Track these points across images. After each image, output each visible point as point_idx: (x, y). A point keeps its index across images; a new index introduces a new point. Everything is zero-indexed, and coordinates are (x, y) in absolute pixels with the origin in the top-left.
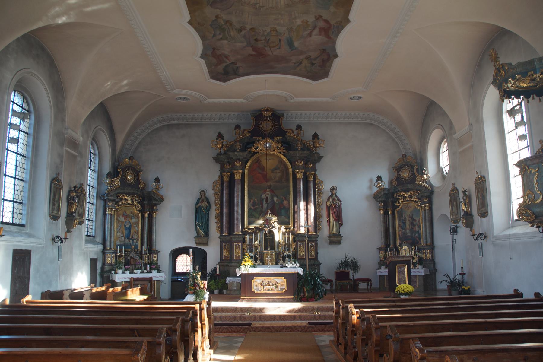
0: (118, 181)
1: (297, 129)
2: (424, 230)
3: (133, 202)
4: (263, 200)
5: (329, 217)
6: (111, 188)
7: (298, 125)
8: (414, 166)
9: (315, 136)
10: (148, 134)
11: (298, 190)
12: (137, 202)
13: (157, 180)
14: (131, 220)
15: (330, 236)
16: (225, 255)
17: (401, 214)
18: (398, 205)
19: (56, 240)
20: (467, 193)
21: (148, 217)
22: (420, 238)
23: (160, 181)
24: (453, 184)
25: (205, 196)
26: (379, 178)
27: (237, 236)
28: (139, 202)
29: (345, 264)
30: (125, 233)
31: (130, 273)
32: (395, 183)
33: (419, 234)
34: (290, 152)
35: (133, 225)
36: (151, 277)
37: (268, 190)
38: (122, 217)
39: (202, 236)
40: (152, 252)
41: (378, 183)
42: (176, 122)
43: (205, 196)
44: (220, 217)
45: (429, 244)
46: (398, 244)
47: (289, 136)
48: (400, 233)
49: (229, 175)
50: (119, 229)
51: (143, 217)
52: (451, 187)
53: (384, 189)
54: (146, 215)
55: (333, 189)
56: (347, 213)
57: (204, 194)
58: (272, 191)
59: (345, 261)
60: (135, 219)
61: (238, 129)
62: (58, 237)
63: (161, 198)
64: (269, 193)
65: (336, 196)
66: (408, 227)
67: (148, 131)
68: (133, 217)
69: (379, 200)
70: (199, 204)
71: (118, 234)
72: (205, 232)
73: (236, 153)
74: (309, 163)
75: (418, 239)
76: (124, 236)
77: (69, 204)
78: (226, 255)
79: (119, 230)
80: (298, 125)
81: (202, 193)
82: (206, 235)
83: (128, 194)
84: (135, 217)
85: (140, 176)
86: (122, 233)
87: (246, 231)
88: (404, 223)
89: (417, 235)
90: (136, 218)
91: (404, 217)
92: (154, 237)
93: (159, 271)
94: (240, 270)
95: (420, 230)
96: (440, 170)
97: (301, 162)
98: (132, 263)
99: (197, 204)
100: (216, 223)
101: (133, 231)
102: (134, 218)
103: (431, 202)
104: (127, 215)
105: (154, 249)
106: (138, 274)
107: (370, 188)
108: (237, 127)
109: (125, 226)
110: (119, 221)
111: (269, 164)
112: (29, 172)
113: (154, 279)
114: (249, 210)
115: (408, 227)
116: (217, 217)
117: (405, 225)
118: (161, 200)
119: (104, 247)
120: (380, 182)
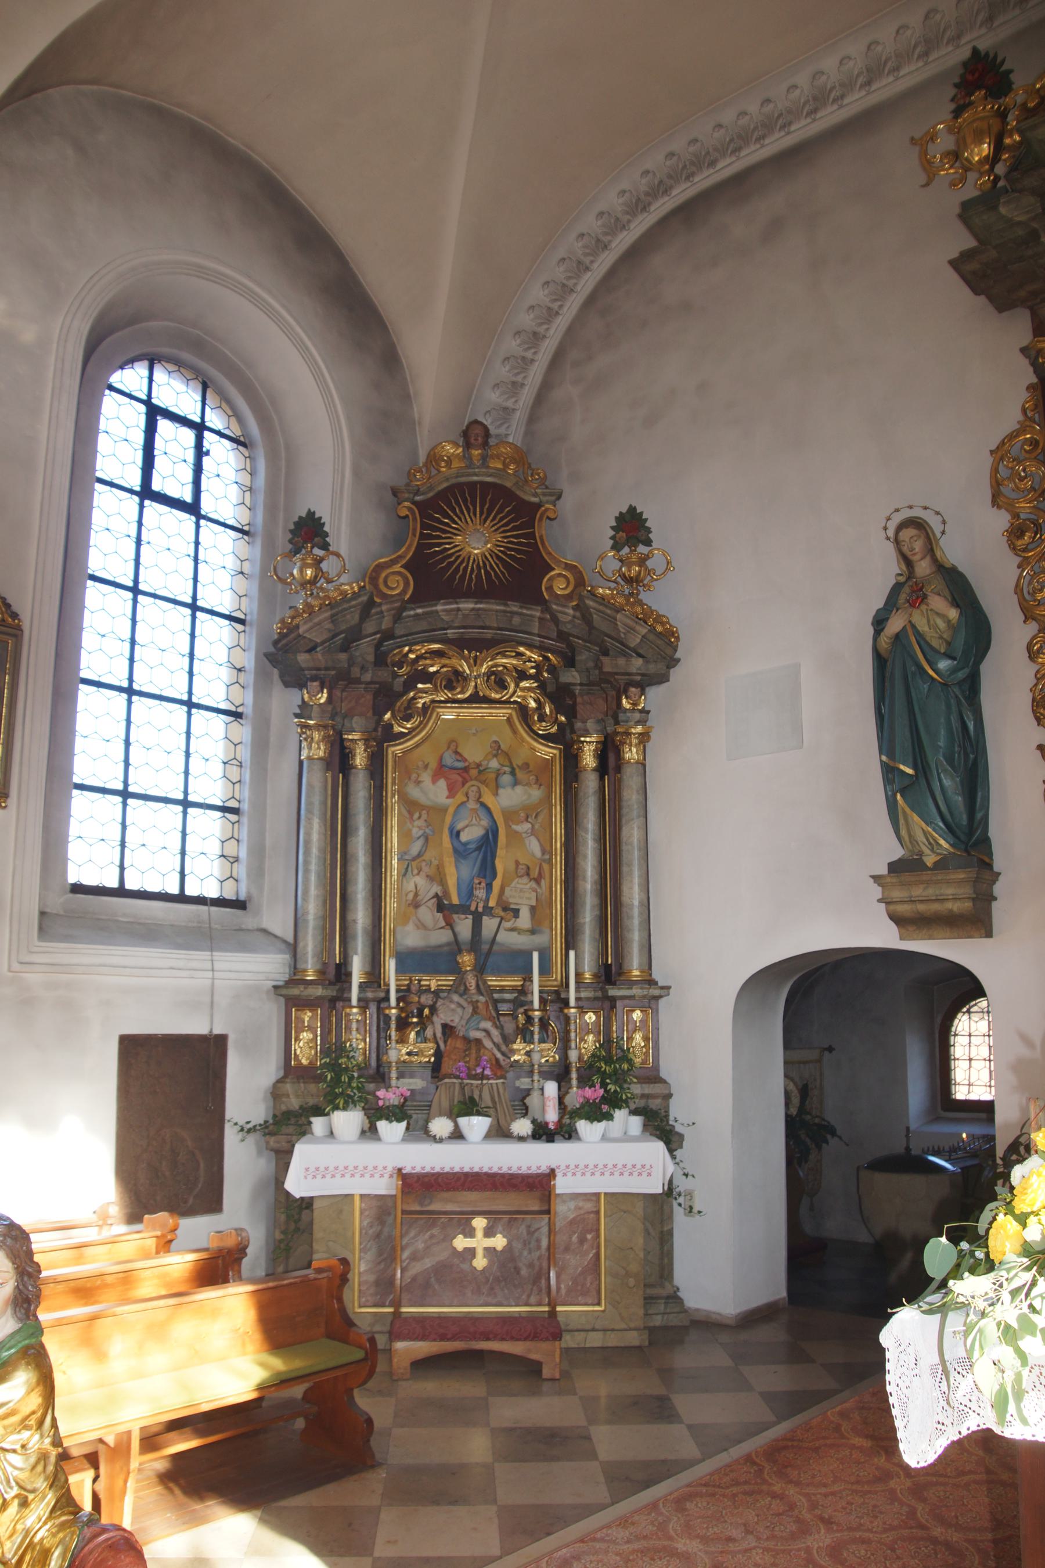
10: (591, 300)
12: (525, 684)
14: (496, 794)
21: (602, 769)
23: (648, 530)
25: (935, 560)
35: (508, 827)
38: (434, 781)
39: (930, 860)
42: (727, 167)
43: (935, 560)
50: (416, 848)
54: (589, 759)
57: (918, 545)
60: (519, 789)
63: (659, 635)
67: (588, 283)
68: (506, 779)
70: (895, 624)
71: (410, 886)
72: (951, 829)
79: (414, 859)
81: (907, 534)
82: (967, 851)
84: (520, 774)
86: (438, 876)
90: (528, 784)
92: (632, 893)
99: (879, 622)
101: (512, 867)
102: (516, 783)
104: (466, 769)
109: (456, 834)
110: (411, 806)
113: (562, 1185)
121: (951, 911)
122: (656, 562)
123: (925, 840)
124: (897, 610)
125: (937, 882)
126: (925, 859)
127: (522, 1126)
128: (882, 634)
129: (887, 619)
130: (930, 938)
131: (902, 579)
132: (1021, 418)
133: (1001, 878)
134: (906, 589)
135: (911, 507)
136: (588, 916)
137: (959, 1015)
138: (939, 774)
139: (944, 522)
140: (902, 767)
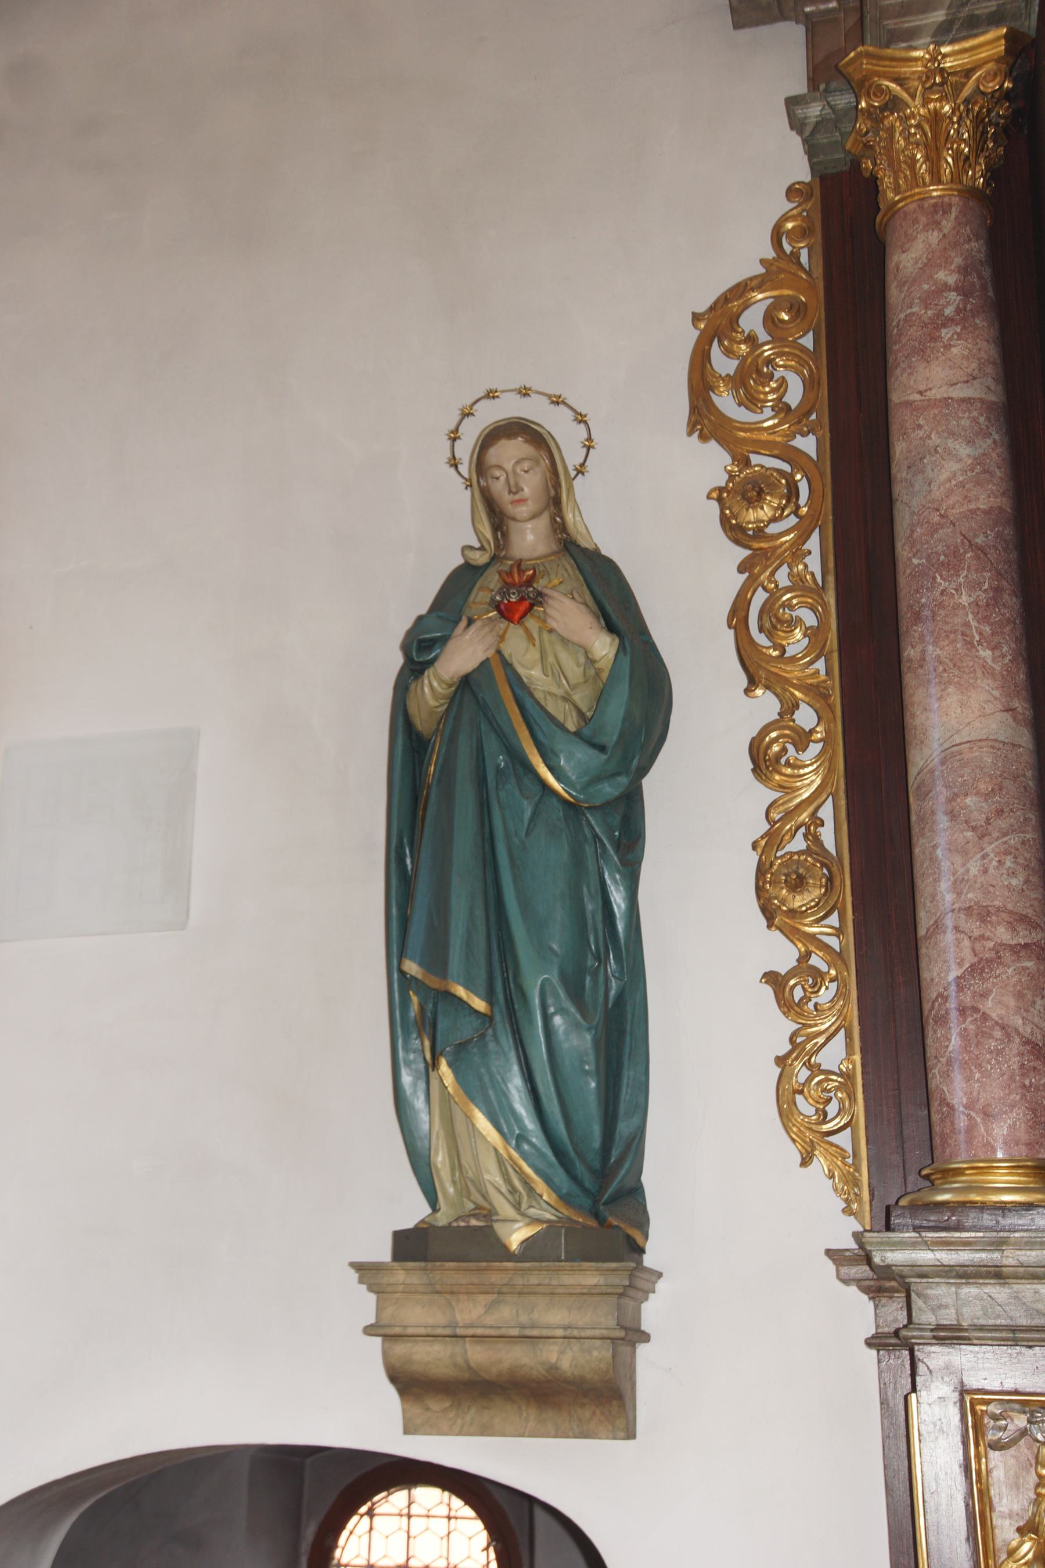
57: (531, 484)
82: (597, 1216)
100: (772, 978)
121: (553, 1368)
123: (498, 1179)
124: (470, 622)
125: (522, 1293)
126: (500, 1228)
128: (429, 673)
129: (444, 640)
130: (485, 1431)
131: (480, 558)
132: (770, 254)
133: (661, 1285)
134: (492, 580)
135: (524, 392)
137: (355, 1519)
138: (547, 1019)
139: (589, 446)
140: (461, 992)
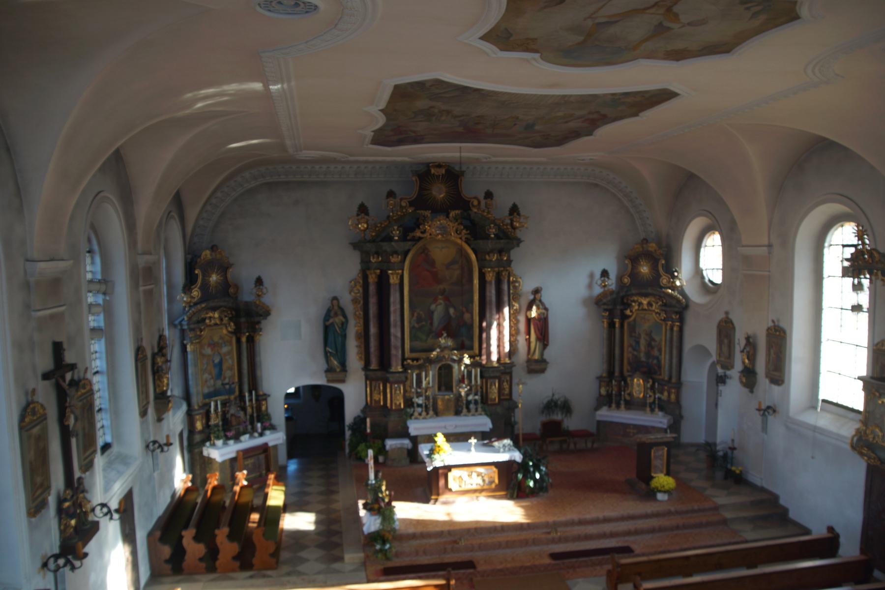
0: (196, 291)
1: (485, 198)
2: (667, 357)
3: (221, 320)
4: (433, 312)
5: (529, 333)
6: (193, 312)
7: (488, 191)
8: (659, 260)
9: (514, 210)
11: (488, 299)
13: (259, 281)
15: (529, 361)
16: (375, 400)
17: (632, 328)
18: (630, 314)
19: (151, 447)
20: (751, 340)
22: (660, 367)
24: (727, 313)
26: (605, 274)
27: (398, 375)
28: (231, 319)
29: (551, 406)
30: (215, 372)
31: (235, 443)
32: (626, 280)
33: (659, 361)
34: (481, 242)
36: (266, 444)
37: (440, 297)
39: (338, 370)
40: (262, 398)
41: (603, 281)
44: (364, 337)
45: (674, 380)
46: (626, 373)
47: (475, 213)
48: (630, 355)
49: (378, 274)
51: (239, 341)
52: (722, 316)
53: (612, 292)
54: (244, 339)
55: (537, 291)
56: (555, 327)
58: (447, 299)
59: (552, 400)
61: (391, 199)
62: (155, 442)
64: (441, 301)
65: (540, 301)
66: (643, 347)
68: (223, 345)
69: (602, 307)
70: (331, 321)
73: (393, 243)
74: (504, 253)
75: (656, 368)
76: (212, 378)
77: (156, 377)
78: (377, 399)
80: (488, 191)
81: (335, 302)
83: (214, 309)
85: (229, 276)
86: (210, 374)
87: (409, 364)
88: (638, 343)
89: (655, 362)
91: (637, 332)
92: (258, 373)
93: (273, 428)
94: (432, 461)
95: (661, 354)
96: (698, 272)
97: (494, 256)
98: (234, 423)
102: (225, 346)
103: (682, 320)
105: (261, 393)
106: (247, 442)
107: (590, 286)
108: (391, 194)
109: (213, 361)
111: (441, 254)
112: (104, 356)
114: (412, 328)
115: (643, 347)
116: (358, 337)
117: (639, 346)
118: (266, 313)
119: (189, 405)
120: (606, 279)
122: (264, 291)
127: (256, 434)
136: (246, 380)
